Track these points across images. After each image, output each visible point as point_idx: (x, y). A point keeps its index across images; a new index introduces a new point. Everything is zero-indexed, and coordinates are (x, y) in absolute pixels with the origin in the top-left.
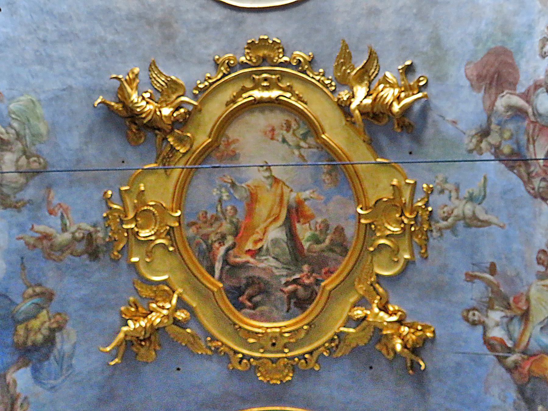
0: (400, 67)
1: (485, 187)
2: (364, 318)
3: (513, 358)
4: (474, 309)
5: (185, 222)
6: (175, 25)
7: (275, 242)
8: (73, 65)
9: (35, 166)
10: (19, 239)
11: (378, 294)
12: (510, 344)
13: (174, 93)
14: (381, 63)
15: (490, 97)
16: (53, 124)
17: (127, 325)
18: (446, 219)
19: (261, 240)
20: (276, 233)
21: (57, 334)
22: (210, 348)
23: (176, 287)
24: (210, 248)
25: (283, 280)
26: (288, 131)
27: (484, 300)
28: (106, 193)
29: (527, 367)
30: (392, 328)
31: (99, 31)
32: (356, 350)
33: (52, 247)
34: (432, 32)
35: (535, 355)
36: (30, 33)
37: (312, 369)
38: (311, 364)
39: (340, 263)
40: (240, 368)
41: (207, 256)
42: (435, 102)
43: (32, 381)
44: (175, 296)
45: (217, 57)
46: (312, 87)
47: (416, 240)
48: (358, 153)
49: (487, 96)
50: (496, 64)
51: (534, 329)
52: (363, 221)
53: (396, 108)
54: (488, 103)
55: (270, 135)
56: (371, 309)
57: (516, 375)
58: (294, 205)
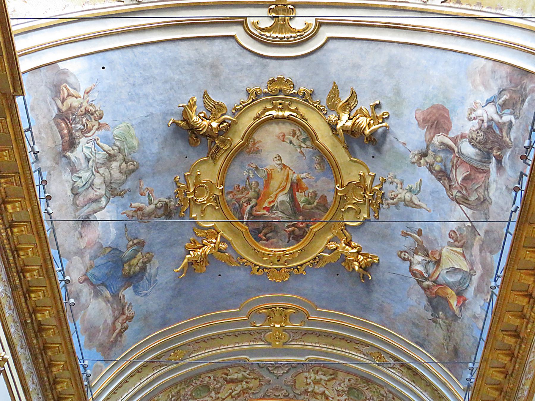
0: (372, 104)
1: (420, 186)
3: (427, 283)
4: (405, 252)
5: (225, 192)
6: (220, 67)
7: (282, 203)
8: (153, 99)
9: (131, 167)
10: (123, 213)
12: (426, 275)
13: (219, 112)
14: (358, 99)
15: (430, 134)
16: (142, 139)
17: (190, 254)
18: (393, 199)
19: (273, 201)
20: (283, 197)
24: (241, 206)
25: (286, 225)
26: (293, 137)
28: (176, 177)
29: (435, 290)
30: (353, 257)
31: (169, 72)
34: (395, 85)
36: (124, 81)
37: (302, 274)
39: (323, 216)
40: (257, 273)
42: (392, 129)
43: (134, 293)
44: (219, 236)
45: (248, 89)
46: (311, 110)
48: (341, 155)
49: (428, 132)
50: (437, 115)
52: (339, 194)
53: (367, 131)
54: (428, 137)
55: (282, 138)
56: (340, 243)
57: (428, 293)
58: (295, 181)
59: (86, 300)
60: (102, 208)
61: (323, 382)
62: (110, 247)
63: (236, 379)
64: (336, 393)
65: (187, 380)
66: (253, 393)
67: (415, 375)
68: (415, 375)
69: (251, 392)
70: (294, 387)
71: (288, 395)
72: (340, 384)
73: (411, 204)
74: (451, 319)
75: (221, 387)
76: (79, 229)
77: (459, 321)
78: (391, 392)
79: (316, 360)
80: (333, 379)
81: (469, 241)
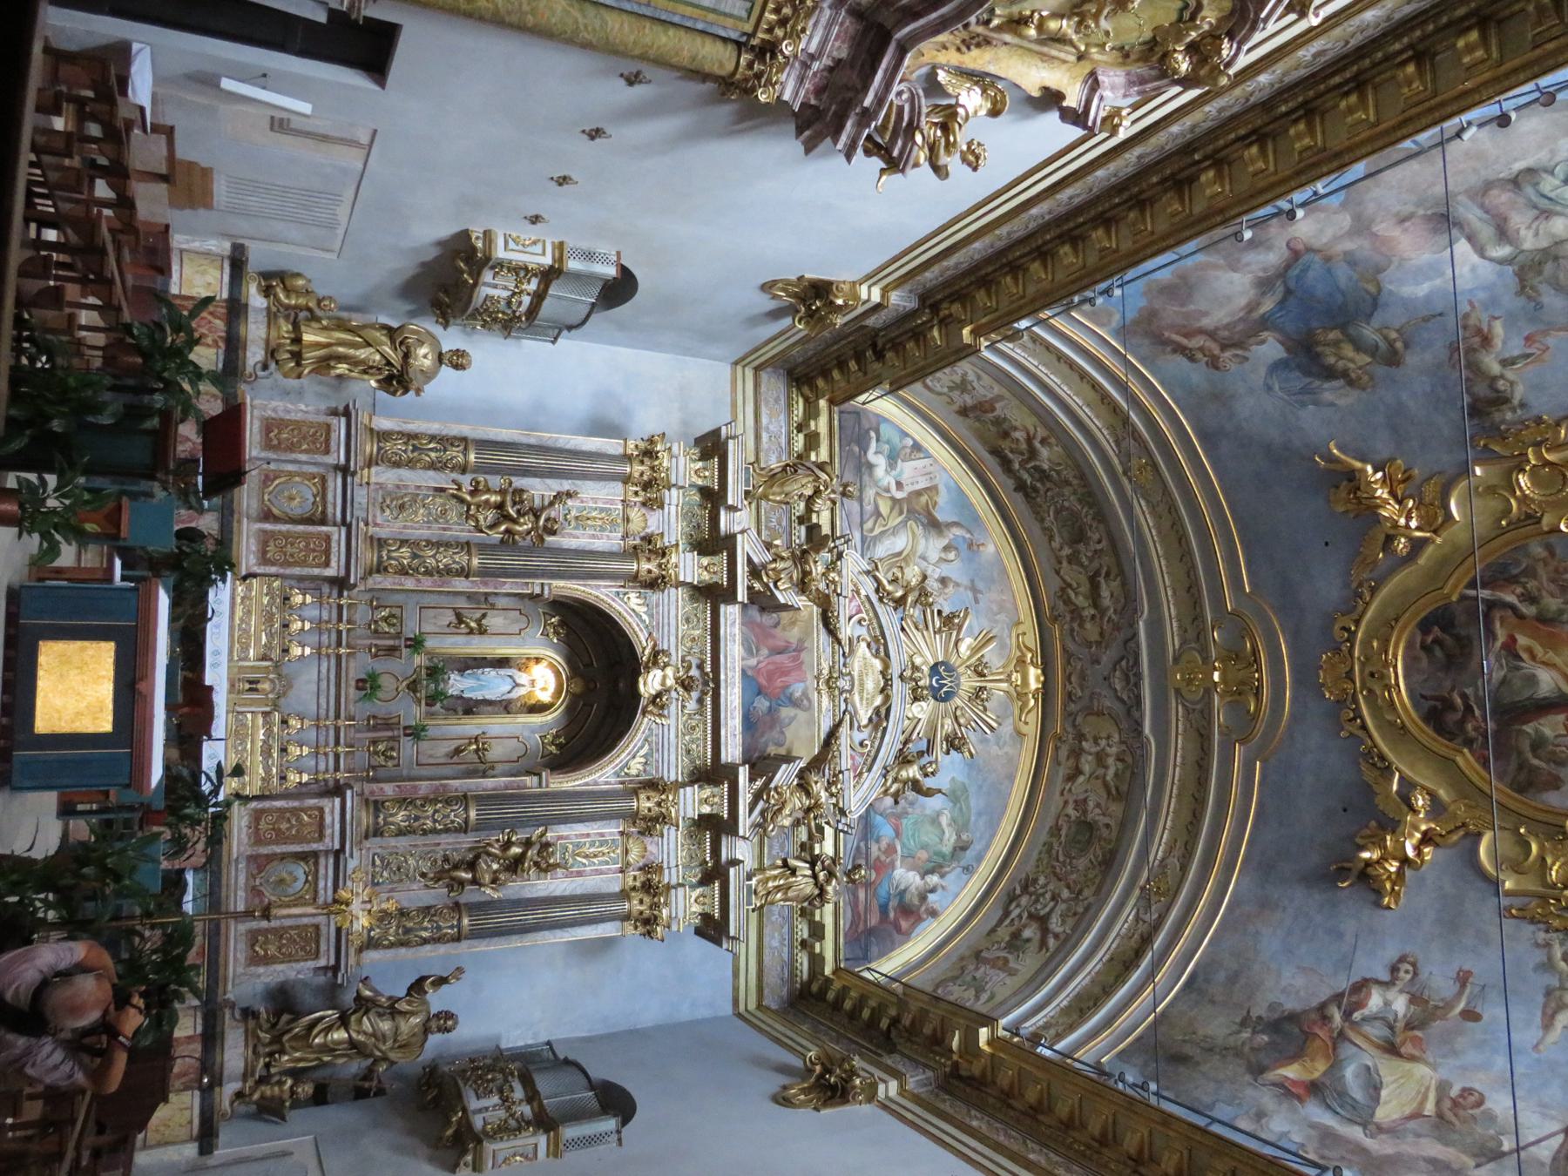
2: (1415, 811)
3: (1337, 1017)
4: (1415, 974)
5: (1553, 539)
7: (1532, 680)
10: (1471, 303)
11: (1449, 832)
12: (1357, 1016)
17: (1375, 471)
21: (1341, 382)
22: (1360, 585)
23: (1445, 534)
24: (1513, 580)
25: (1469, 691)
27: (1426, 992)
32: (1368, 792)
33: (1471, 350)
35: (1334, 1049)
38: (1348, 727)
40: (1337, 627)
41: (1499, 575)
43: (1270, 361)
47: (1533, 904)
51: (1372, 1058)
56: (1428, 819)
57: (1313, 1016)
59: (1248, 264)
60: (1481, 252)
61: (1101, 771)
62: (1380, 290)
63: (1099, 596)
64: (1082, 797)
65: (1091, 495)
66: (1072, 630)
67: (1124, 963)
68: (1124, 963)
69: (1075, 625)
70: (1090, 711)
72: (1098, 805)
73: (1553, 1005)
74: (1252, 1058)
75: (1082, 565)
76: (1421, 212)
77: (1248, 1078)
78: (1087, 909)
79: (1144, 758)
80: (1109, 793)
81: (1456, 1137)
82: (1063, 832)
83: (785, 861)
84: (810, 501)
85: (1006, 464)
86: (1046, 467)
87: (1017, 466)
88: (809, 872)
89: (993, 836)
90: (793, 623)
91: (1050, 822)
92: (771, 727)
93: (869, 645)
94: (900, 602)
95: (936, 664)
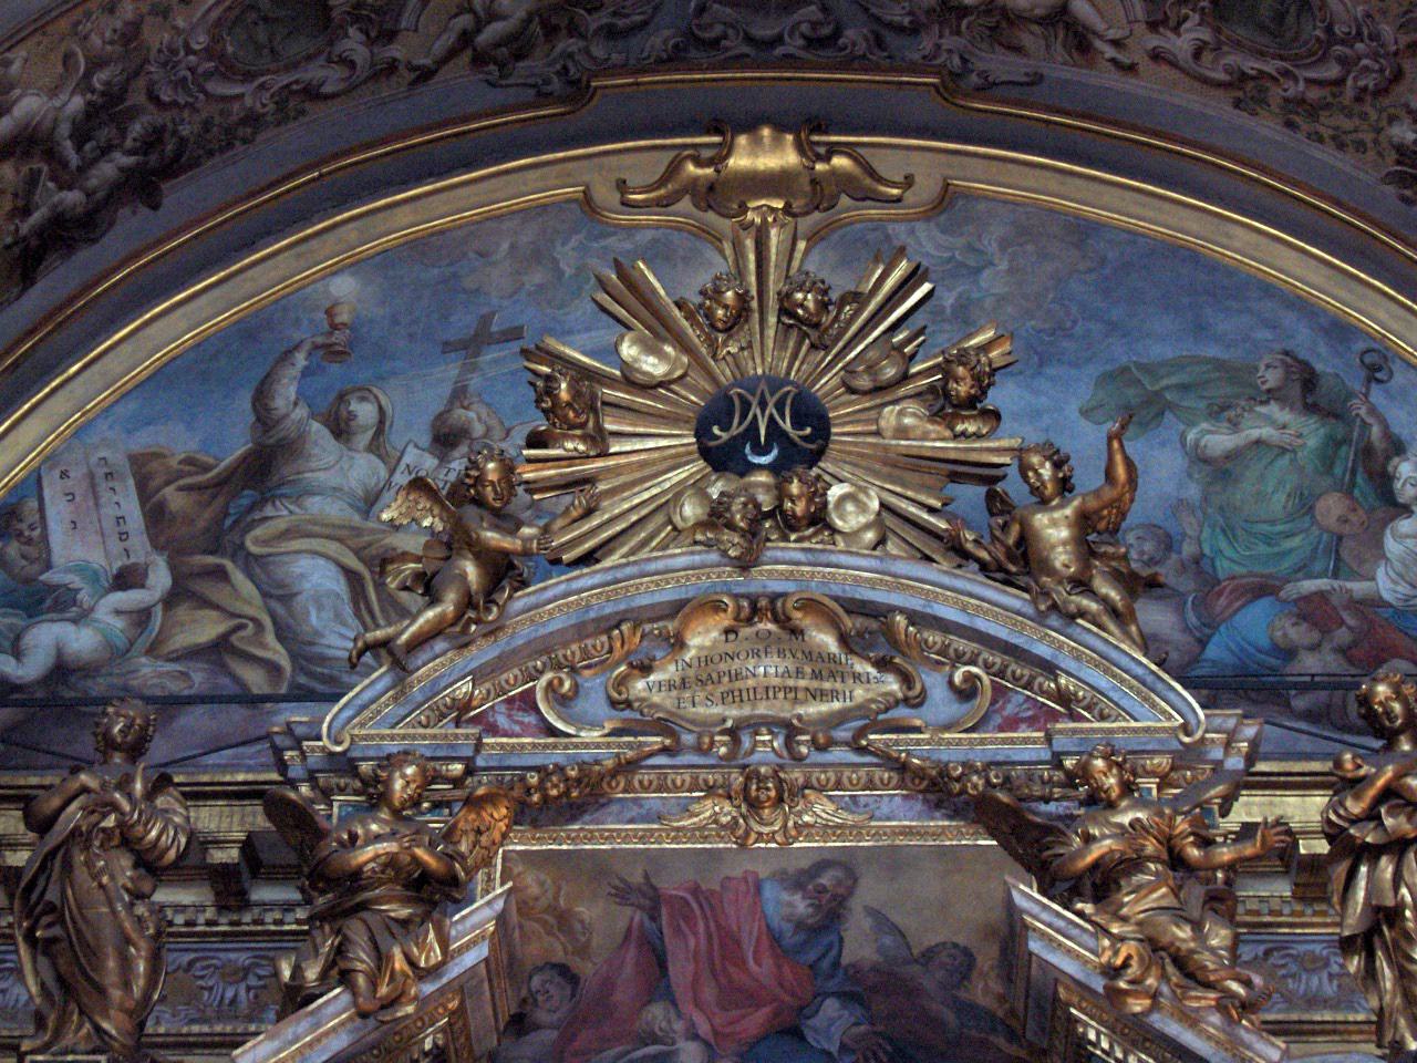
66: (611, 33)
71: (837, 34)
82: (1251, 65)
83: (1347, 945)
84: (151, 865)
85: (64, 234)
86: (77, 103)
87: (73, 197)
88: (1386, 867)
89: (1268, 290)
90: (563, 920)
91: (1219, 107)
92: (914, 992)
93: (645, 669)
94: (503, 572)
95: (705, 453)
